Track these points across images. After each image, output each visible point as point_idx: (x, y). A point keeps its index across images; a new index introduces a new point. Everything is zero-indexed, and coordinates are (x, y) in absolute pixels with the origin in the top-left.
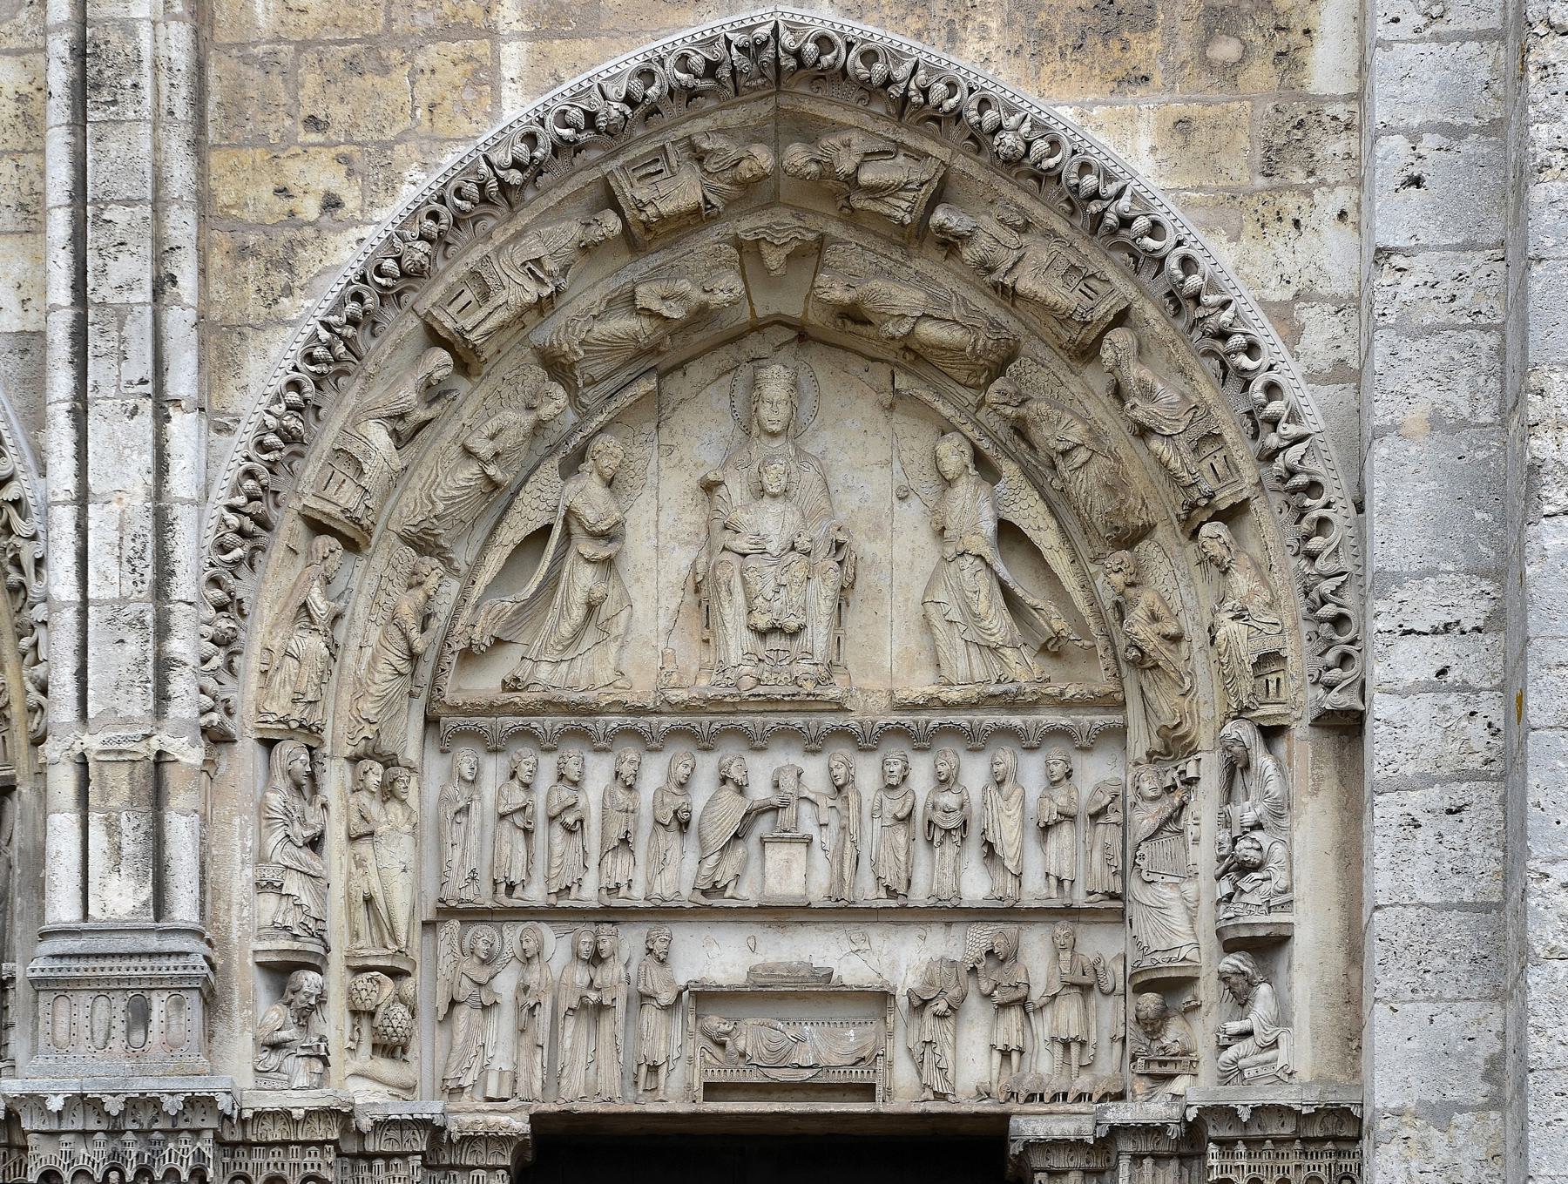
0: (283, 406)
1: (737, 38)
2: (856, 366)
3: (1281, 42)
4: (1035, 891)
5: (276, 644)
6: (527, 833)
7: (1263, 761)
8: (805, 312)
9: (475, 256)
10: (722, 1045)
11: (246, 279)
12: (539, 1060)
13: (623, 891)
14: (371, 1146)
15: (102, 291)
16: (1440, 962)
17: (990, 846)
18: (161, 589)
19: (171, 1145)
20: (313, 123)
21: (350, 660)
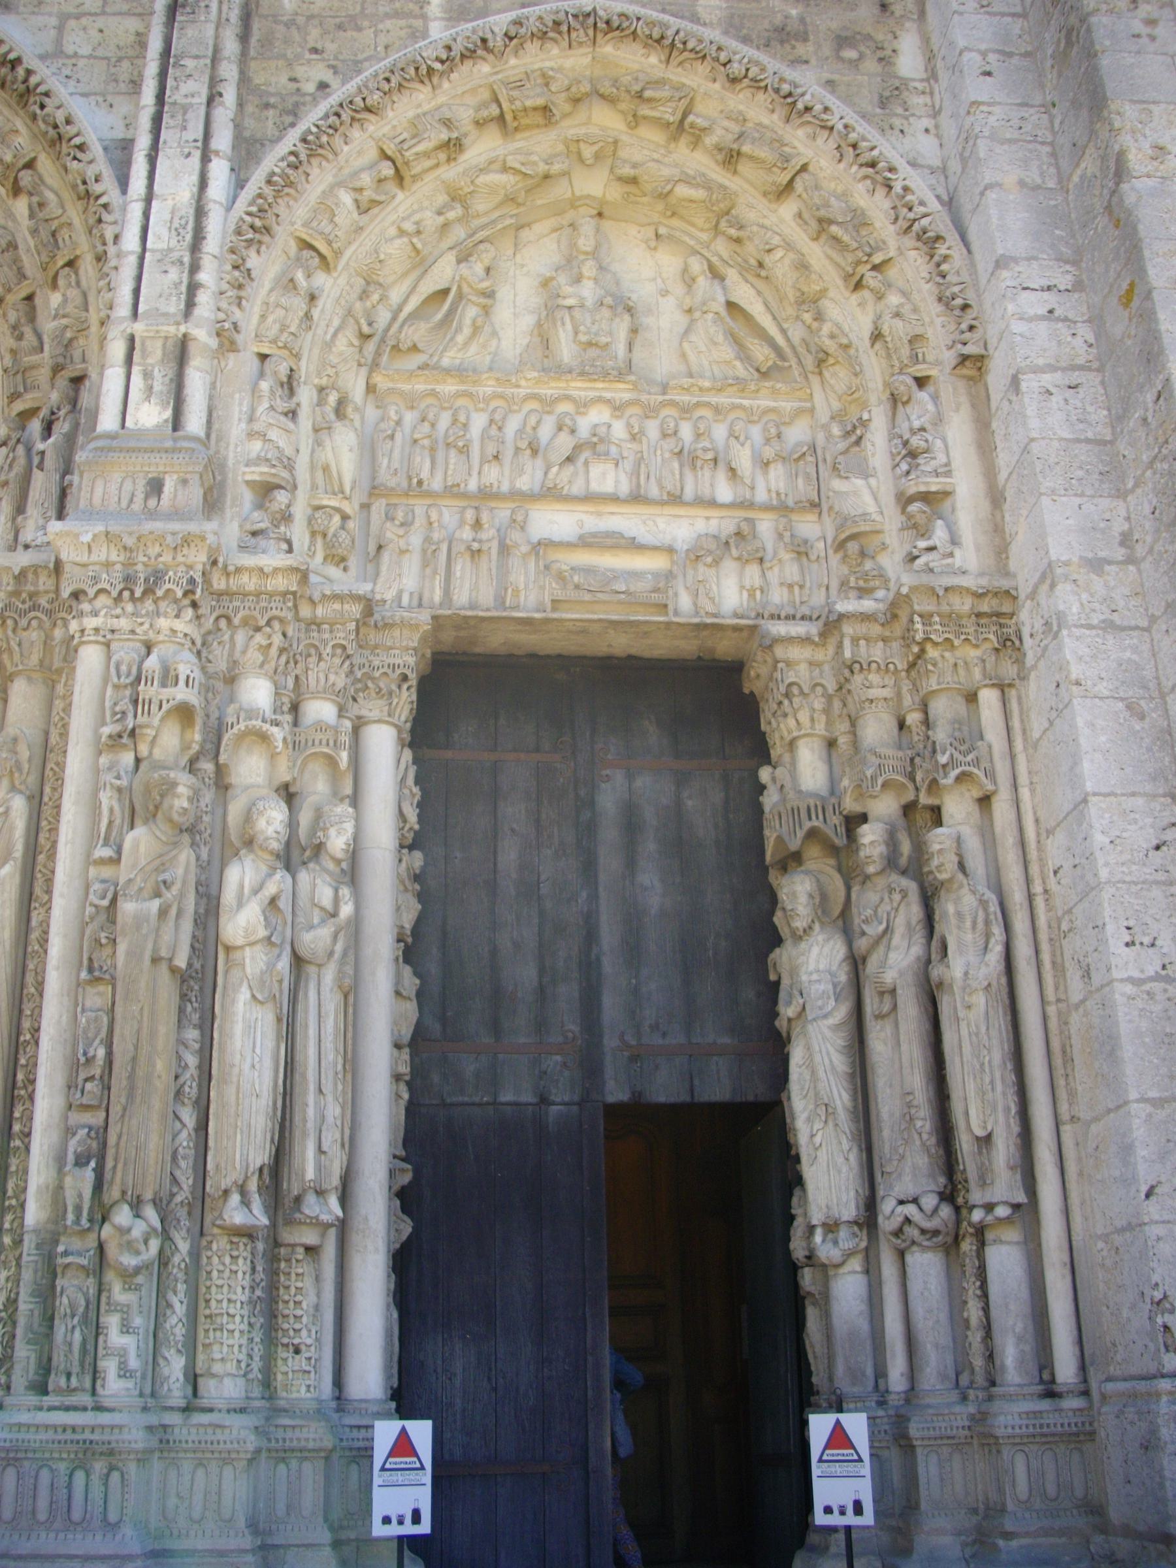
1: (572, 11)
3: (880, 54)
4: (761, 496)
5: (272, 299)
17: (732, 470)
20: (315, 51)
21: (320, 331)
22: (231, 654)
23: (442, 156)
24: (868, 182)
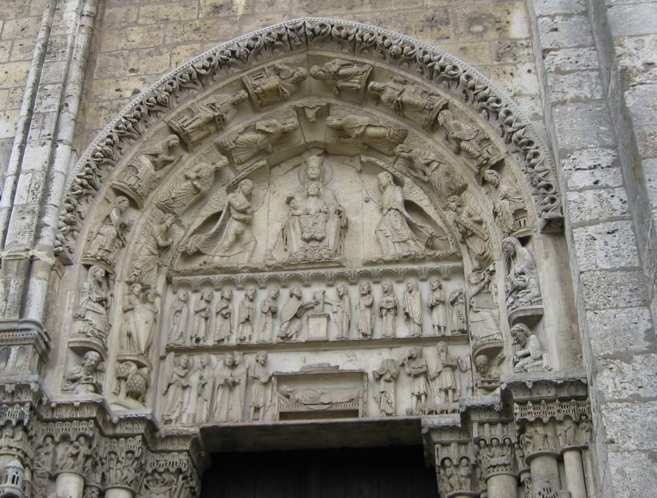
0: (105, 143)
1: (291, 27)
2: (347, 161)
3: (498, 25)
5: (95, 230)
6: (206, 319)
7: (521, 250)
8: (325, 139)
9: (189, 103)
10: (288, 397)
11: (101, 116)
12: (205, 406)
13: (247, 340)
14: (119, 431)
15: (38, 109)
16: (615, 292)
17: (407, 314)
18: (43, 202)
19: (10, 409)
20: (132, 70)
21: (131, 247)
22: (54, 461)
23: (212, 128)
24: (484, 111)
